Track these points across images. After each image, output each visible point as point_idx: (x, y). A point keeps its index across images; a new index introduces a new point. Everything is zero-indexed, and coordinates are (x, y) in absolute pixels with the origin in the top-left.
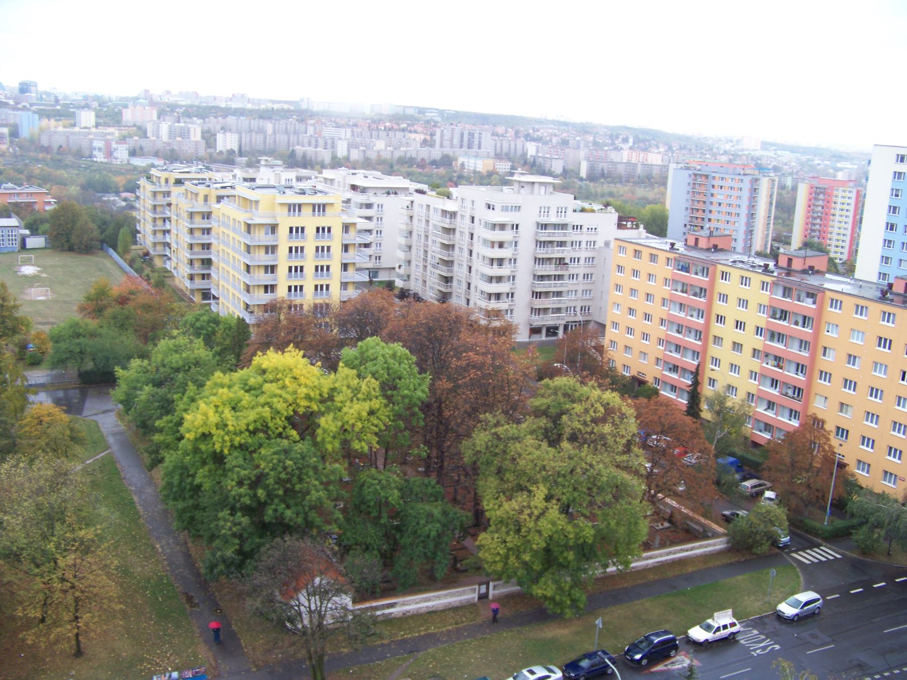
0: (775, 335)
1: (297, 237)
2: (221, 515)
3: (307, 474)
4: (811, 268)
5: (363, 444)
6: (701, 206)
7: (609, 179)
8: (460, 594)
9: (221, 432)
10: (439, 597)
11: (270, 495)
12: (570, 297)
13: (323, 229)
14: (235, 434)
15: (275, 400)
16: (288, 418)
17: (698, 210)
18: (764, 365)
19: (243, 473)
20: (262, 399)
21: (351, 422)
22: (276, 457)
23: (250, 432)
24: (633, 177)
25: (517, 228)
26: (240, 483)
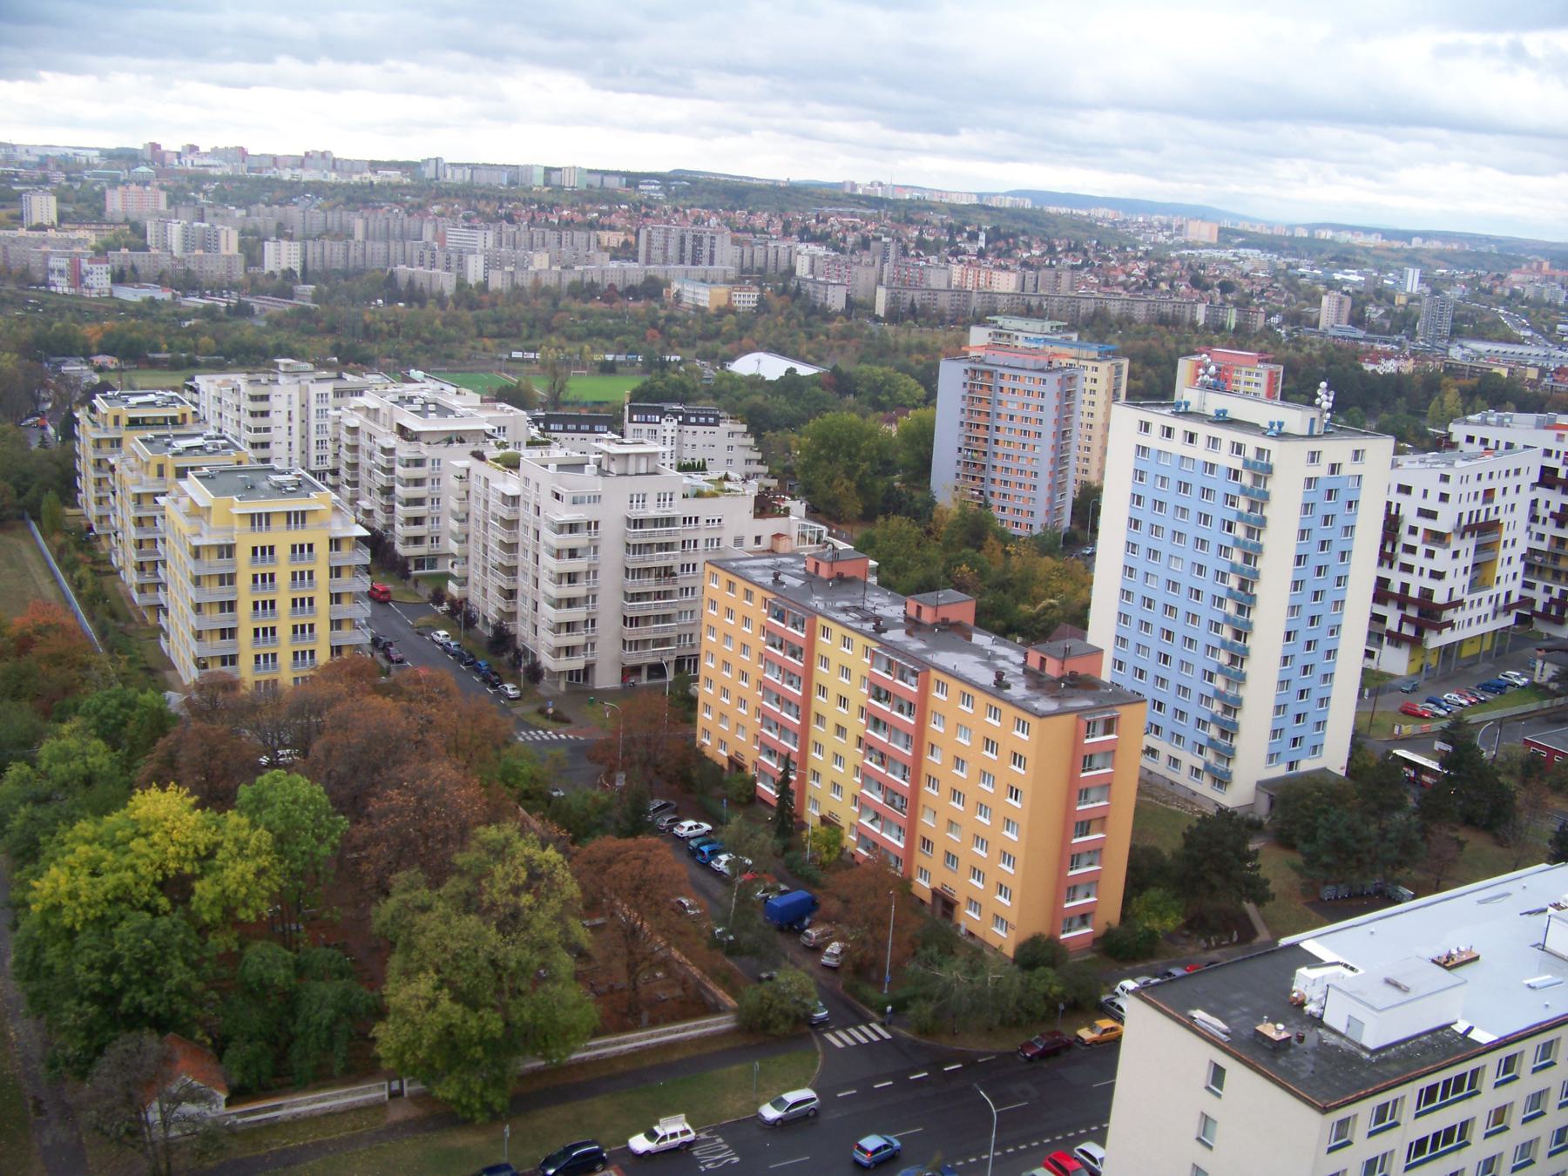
0: (877, 723)
1: (263, 561)
2: (66, 1005)
3: (172, 954)
4: (945, 621)
5: (250, 912)
6: (982, 421)
7: (921, 320)
8: (364, 1092)
9: (73, 904)
10: (337, 1096)
11: (127, 981)
12: (683, 621)
13: (302, 547)
14: (90, 906)
15: (139, 862)
16: (155, 883)
17: (978, 426)
18: (867, 761)
19: (95, 955)
20: (127, 860)
21: (234, 886)
22: (133, 935)
23: (109, 902)
24: (965, 314)
25: (596, 526)
26: (91, 968)
